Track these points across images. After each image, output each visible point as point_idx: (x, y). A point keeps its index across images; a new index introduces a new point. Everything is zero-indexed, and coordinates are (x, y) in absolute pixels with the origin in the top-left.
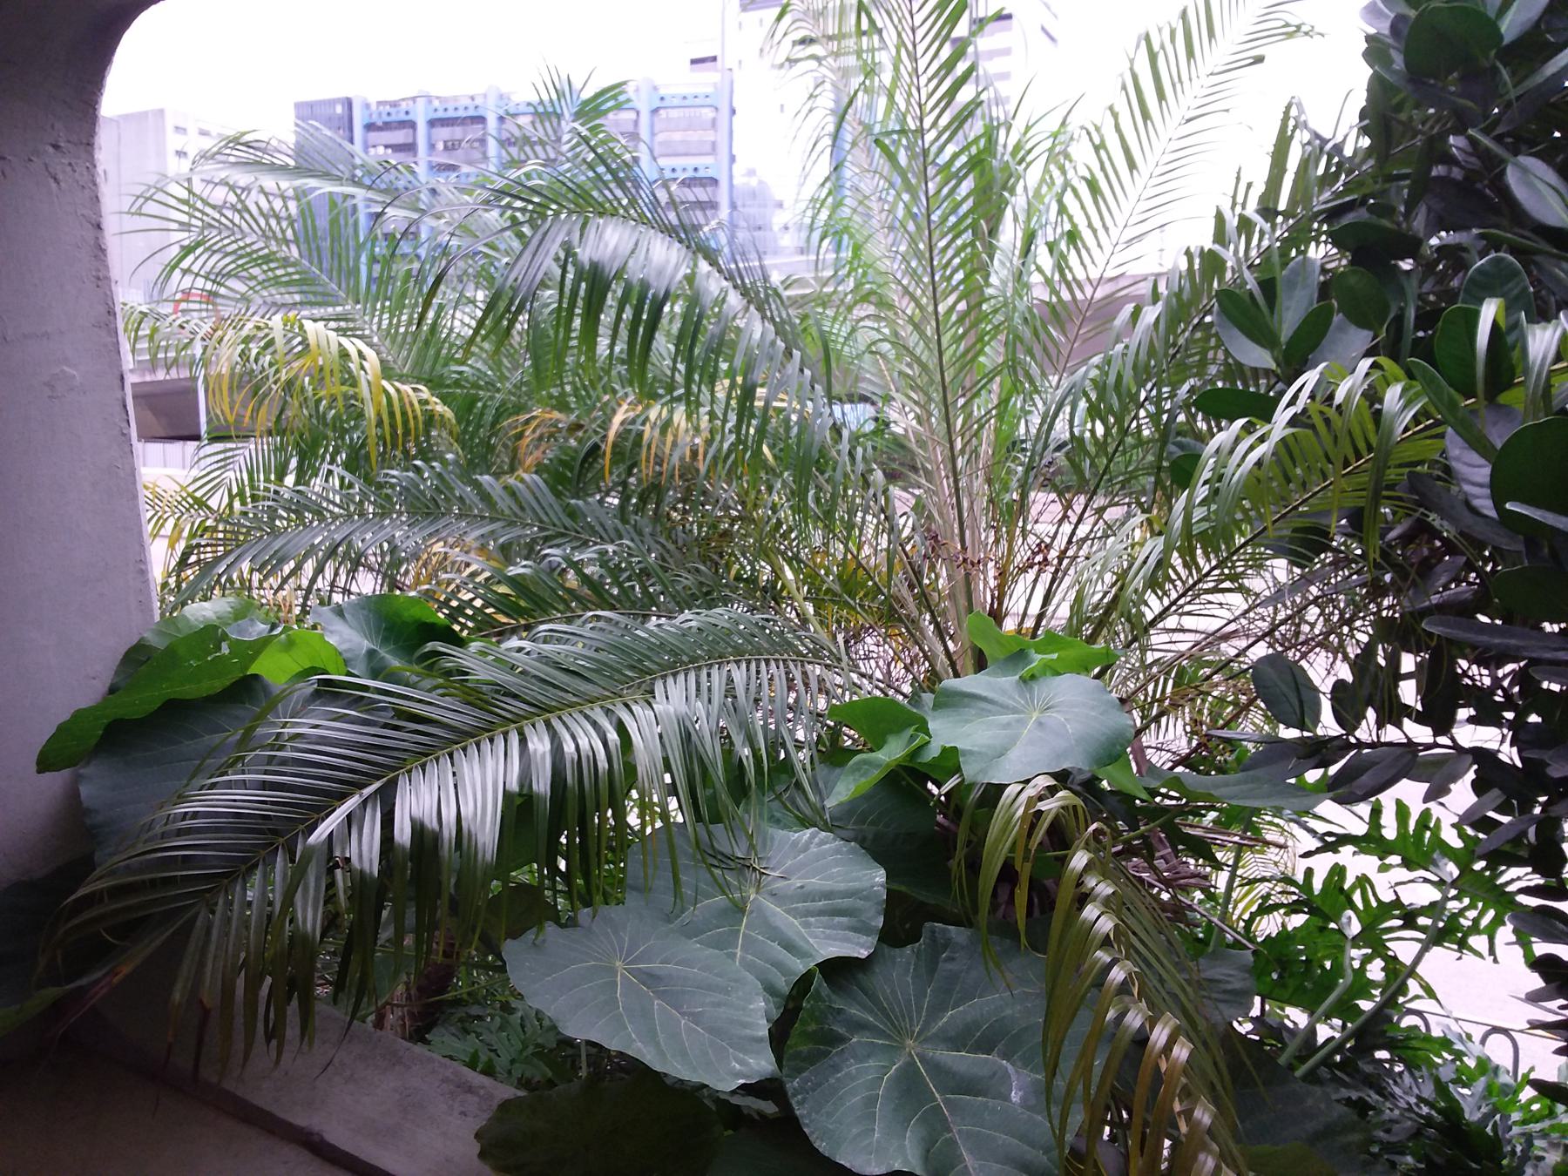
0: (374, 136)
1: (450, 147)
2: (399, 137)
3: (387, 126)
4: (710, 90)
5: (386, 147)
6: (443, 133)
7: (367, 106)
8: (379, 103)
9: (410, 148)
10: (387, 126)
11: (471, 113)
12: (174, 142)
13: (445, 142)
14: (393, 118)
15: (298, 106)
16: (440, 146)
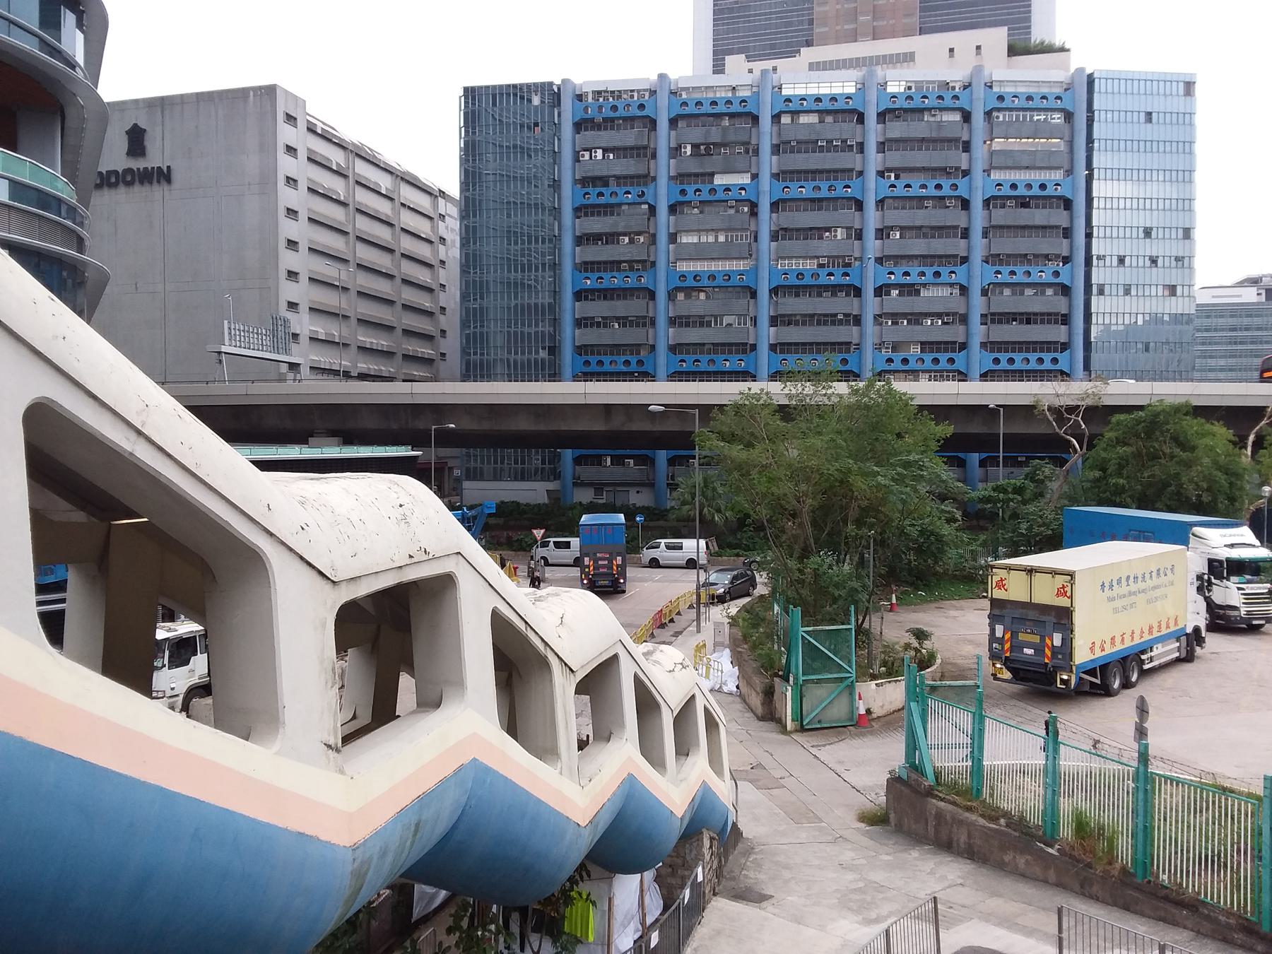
0: (589, 136)
1: (703, 150)
2: (628, 137)
3: (609, 123)
4: (1057, 90)
5: (605, 150)
6: (696, 134)
7: (580, 97)
8: (598, 93)
9: (645, 152)
10: (609, 123)
11: (736, 108)
12: (287, 135)
13: (695, 147)
14: (621, 112)
15: (471, 94)
16: (689, 150)
